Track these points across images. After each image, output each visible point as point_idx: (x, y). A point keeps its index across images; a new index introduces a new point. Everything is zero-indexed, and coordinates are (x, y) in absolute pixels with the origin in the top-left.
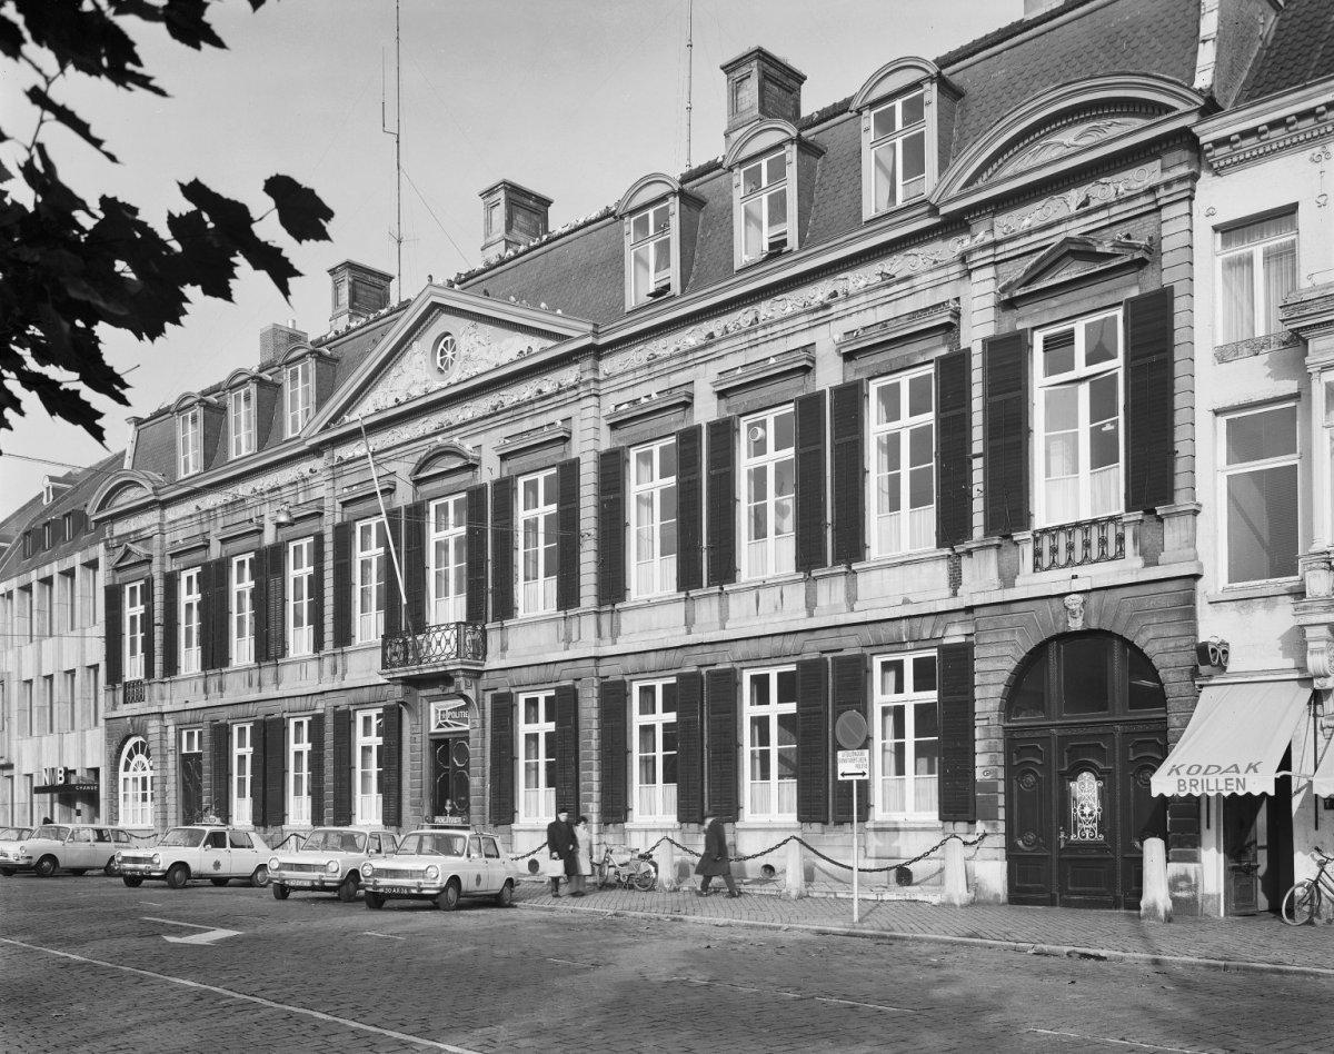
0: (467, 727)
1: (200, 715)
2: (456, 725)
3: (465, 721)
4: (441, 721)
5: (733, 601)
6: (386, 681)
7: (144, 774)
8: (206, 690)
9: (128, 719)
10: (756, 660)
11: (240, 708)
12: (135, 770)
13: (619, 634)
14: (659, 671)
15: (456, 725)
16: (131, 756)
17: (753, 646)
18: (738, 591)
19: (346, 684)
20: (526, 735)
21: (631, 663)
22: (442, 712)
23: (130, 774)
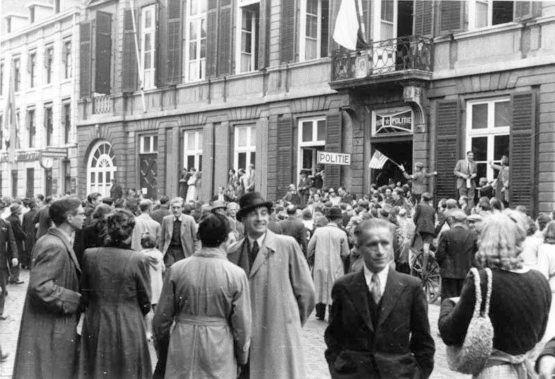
4: (384, 126)
7: (108, 169)
8: (162, 104)
9: (97, 126)
11: (192, 118)
12: (100, 166)
16: (97, 155)
19: (291, 95)
22: (386, 119)
23: (97, 170)
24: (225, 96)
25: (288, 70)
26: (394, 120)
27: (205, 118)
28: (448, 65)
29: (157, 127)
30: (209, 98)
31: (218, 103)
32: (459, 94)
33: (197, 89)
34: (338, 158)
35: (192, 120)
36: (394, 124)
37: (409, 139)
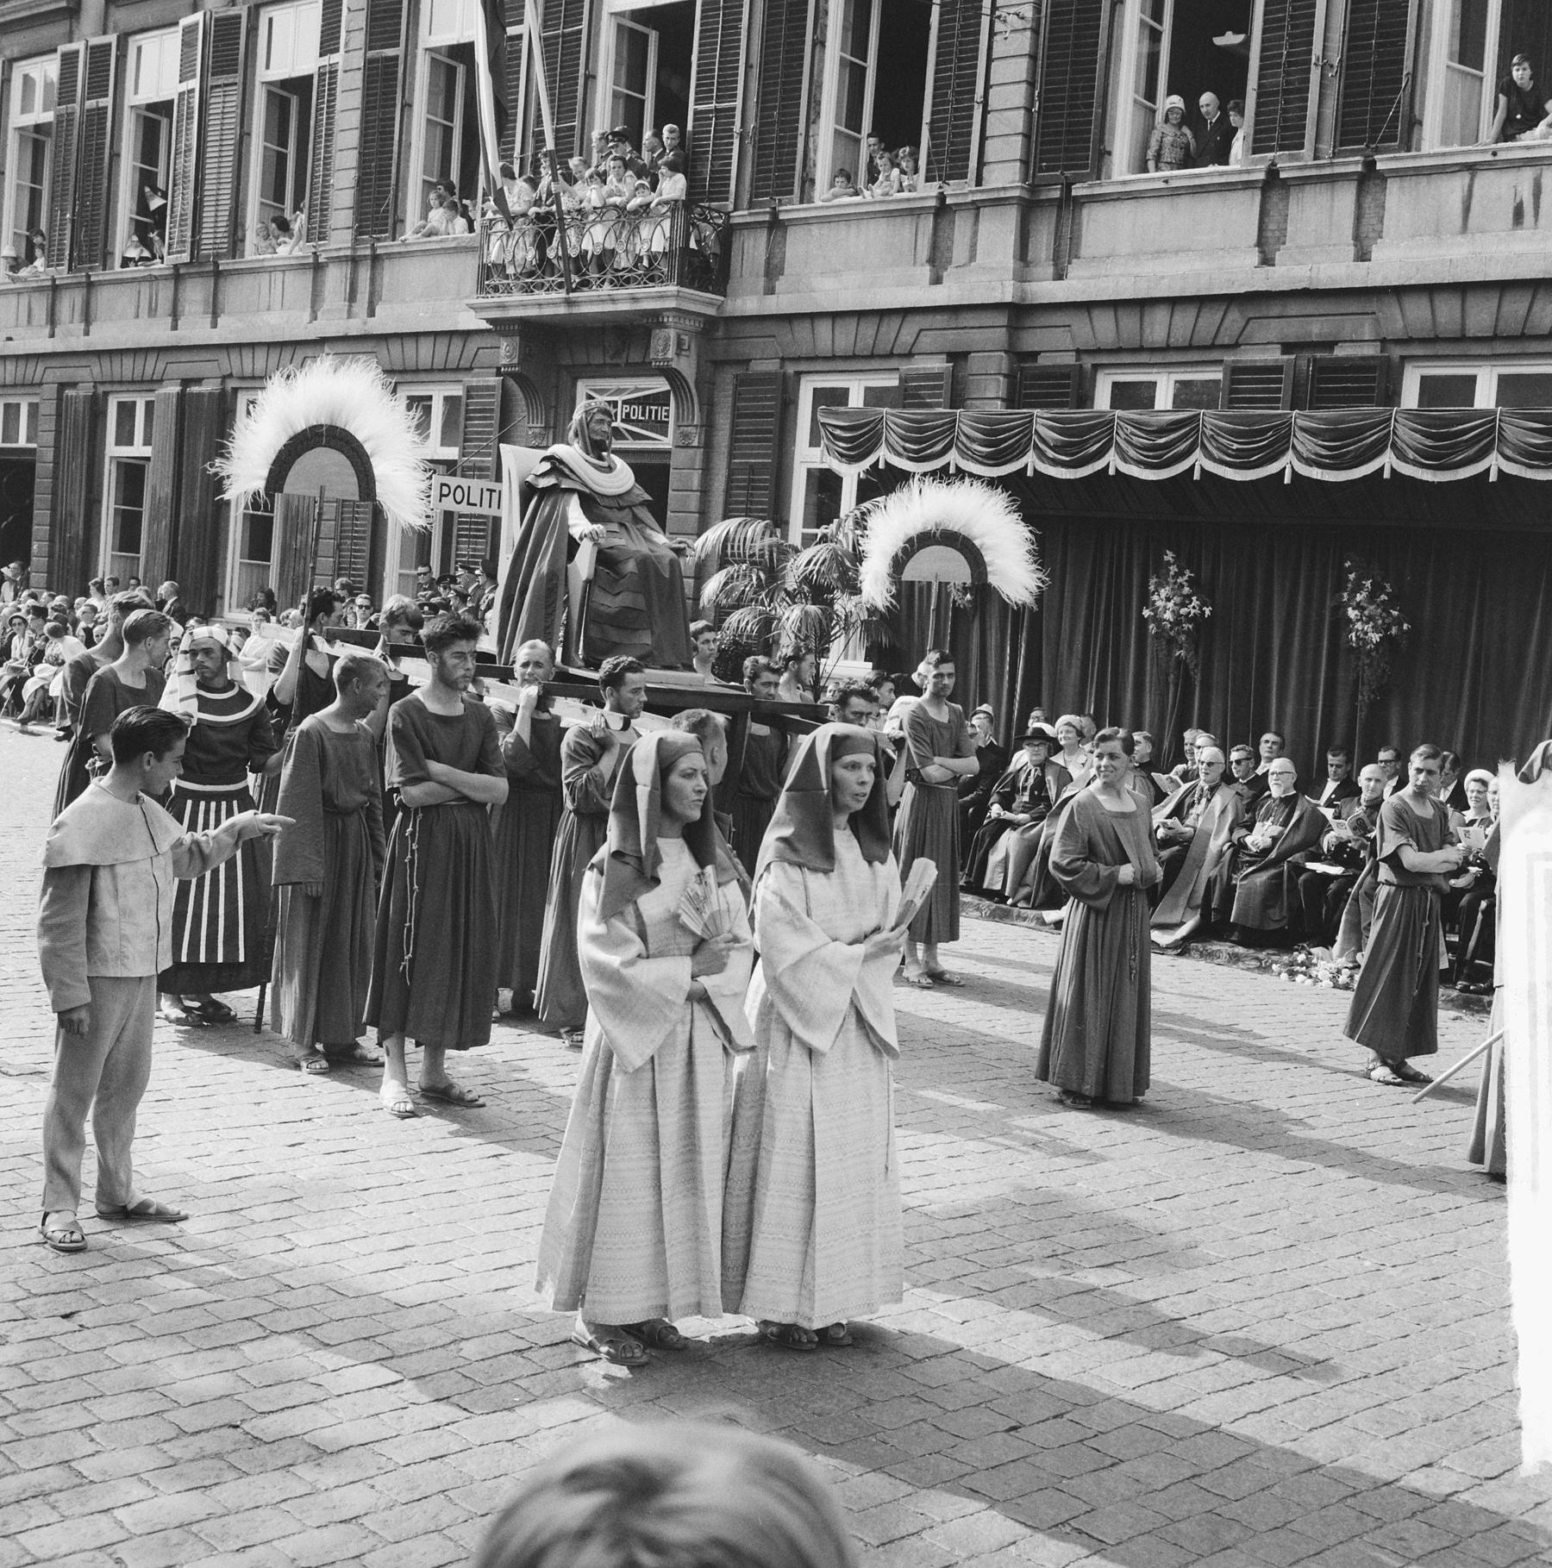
0: (666, 442)
1: (36, 371)
2: (636, 436)
3: (661, 427)
5: (1397, 200)
6: (485, 325)
8: (52, 320)
10: (1435, 342)
11: (128, 362)
13: (1074, 254)
14: (1166, 353)
15: (636, 436)
17: (1447, 311)
18: (1418, 172)
19: (377, 326)
20: (809, 471)
21: (1104, 328)
24: (215, 312)
25: (376, 259)
26: (627, 409)
27: (161, 366)
28: (762, 282)
29: (37, 380)
30: (175, 314)
31: (197, 329)
32: (783, 359)
33: (145, 288)
34: (486, 495)
35: (127, 368)
36: (627, 420)
37: (656, 461)
